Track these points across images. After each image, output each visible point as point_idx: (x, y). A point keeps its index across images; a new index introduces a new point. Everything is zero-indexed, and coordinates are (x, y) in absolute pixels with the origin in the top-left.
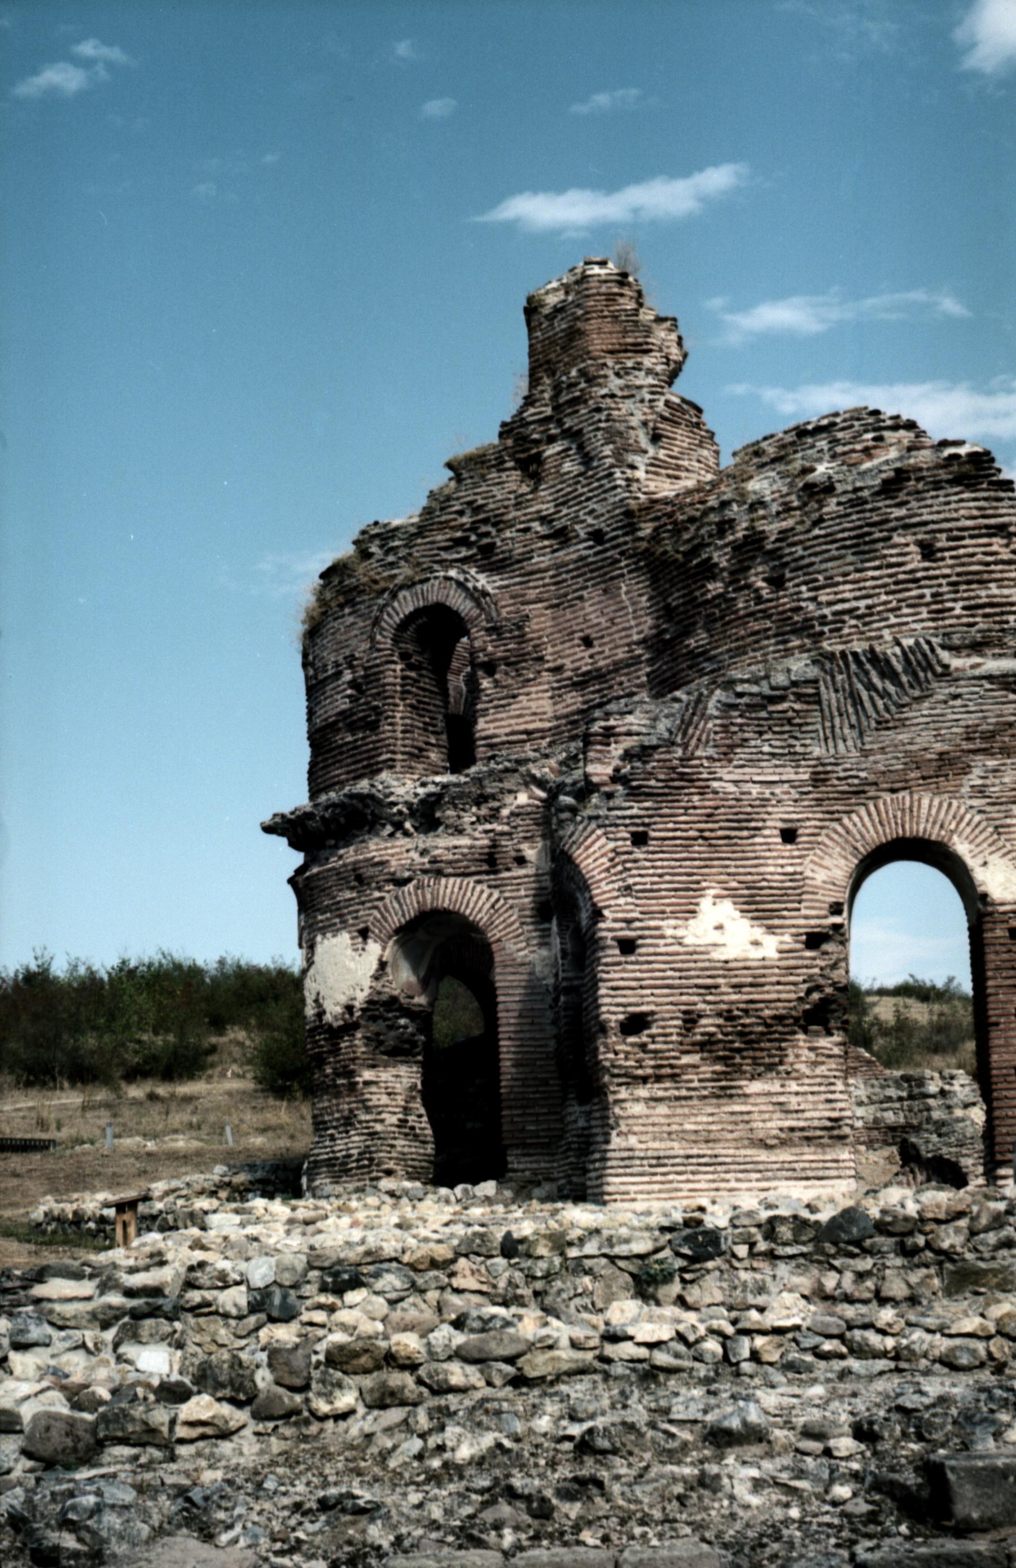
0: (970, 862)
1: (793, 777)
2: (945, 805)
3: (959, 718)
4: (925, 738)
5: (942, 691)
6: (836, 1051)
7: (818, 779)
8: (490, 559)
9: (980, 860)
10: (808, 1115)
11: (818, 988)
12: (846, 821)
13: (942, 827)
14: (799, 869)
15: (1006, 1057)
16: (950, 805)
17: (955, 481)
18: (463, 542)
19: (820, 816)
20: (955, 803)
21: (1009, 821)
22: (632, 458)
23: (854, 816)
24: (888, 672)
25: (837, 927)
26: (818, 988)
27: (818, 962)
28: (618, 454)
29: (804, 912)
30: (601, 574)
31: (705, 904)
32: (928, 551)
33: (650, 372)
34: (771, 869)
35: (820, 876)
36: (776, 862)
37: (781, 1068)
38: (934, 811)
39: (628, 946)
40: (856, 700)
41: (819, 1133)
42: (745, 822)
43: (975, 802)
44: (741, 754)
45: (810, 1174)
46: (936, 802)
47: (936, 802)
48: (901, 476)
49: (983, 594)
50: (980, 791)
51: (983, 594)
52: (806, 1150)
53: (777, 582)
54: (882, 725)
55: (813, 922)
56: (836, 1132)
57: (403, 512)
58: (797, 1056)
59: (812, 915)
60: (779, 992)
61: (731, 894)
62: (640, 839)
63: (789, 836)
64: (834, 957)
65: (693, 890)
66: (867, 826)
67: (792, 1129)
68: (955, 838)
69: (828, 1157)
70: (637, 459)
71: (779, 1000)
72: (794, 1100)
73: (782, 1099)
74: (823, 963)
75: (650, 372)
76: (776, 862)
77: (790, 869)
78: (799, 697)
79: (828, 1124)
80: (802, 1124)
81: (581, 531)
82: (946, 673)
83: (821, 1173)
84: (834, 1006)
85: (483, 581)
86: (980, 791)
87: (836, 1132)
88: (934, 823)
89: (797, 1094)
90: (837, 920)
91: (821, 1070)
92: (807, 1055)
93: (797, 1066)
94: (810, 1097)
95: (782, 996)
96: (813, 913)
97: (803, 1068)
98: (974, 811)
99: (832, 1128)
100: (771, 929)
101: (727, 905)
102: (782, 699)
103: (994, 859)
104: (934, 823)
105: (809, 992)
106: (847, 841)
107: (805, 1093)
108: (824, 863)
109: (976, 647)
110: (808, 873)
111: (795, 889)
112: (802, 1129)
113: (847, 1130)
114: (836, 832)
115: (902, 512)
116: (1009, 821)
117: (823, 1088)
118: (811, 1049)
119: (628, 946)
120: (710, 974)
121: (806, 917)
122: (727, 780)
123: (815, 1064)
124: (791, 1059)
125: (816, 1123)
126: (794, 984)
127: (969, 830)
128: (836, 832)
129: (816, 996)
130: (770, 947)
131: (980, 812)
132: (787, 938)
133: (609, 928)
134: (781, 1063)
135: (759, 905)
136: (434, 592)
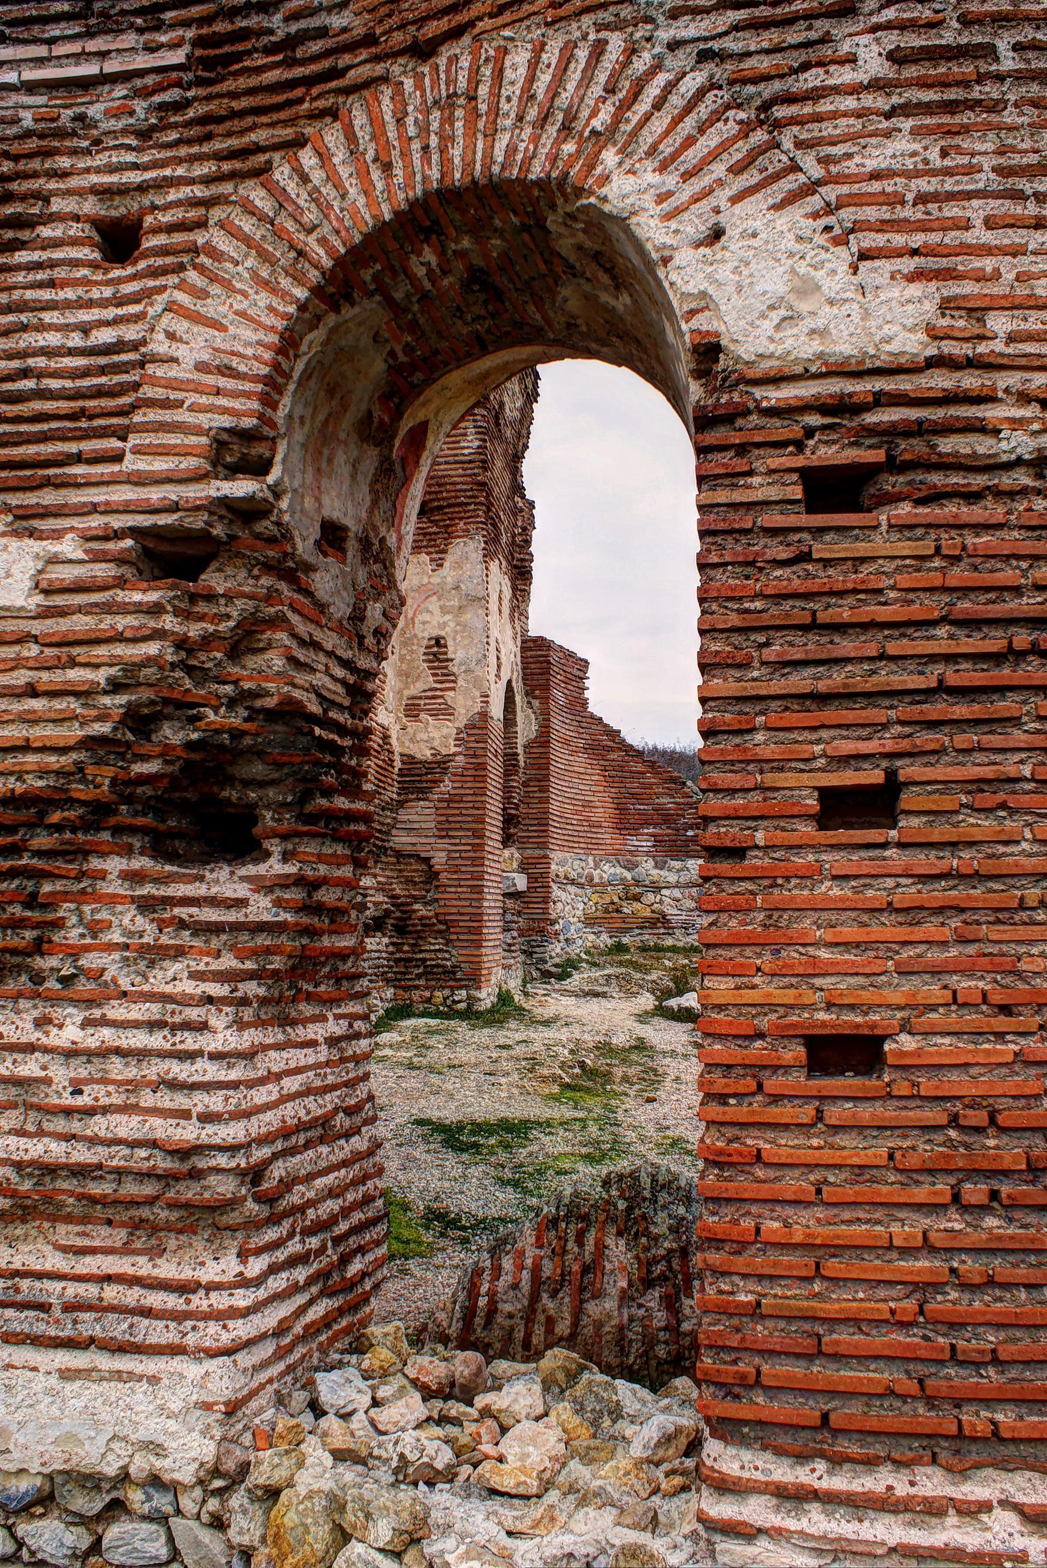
0: (652, 230)
1: (142, 61)
2: (582, 54)
6: (261, 908)
9: (694, 225)
10: (99, 1126)
11: (184, 709)
12: (282, 174)
13: (566, 129)
14: (131, 333)
15: (766, 989)
16: (599, 49)
19: (201, 170)
20: (616, 42)
21: (812, 79)
23: (307, 158)
25: (245, 512)
26: (184, 709)
27: (169, 622)
29: (131, 463)
34: (53, 339)
35: (194, 348)
37: (40, 963)
38: (544, 79)
41: (131, 1188)
43: (689, 29)
45: (89, 1325)
46: (551, 56)
47: (551, 56)
52: (101, 1236)
55: (154, 494)
56: (189, 1191)
58: (95, 928)
59: (157, 475)
60: (32, 719)
63: (118, 241)
64: (236, 610)
67: (49, 1170)
68: (610, 157)
69: (166, 1269)
71: (26, 747)
72: (60, 1074)
73: (30, 1067)
74: (194, 630)
77: (105, 336)
79: (164, 1163)
80: (82, 1155)
83: (118, 1328)
84: (258, 769)
87: (189, 1191)
88: (544, 119)
89: (71, 1053)
90: (242, 487)
91: (174, 977)
92: (127, 922)
93: (90, 961)
94: (117, 1068)
96: (160, 465)
97: (110, 963)
98: (682, 59)
99: (169, 1178)
103: (750, 216)
104: (544, 119)
105: (140, 722)
106: (278, 234)
107: (105, 1052)
108: (211, 308)
110: (159, 345)
112: (81, 1171)
113: (225, 1187)
114: (250, 209)
116: (812, 79)
117: (157, 1040)
118: (146, 906)
121: (139, 480)
123: (155, 955)
124: (73, 935)
125: (118, 1157)
126: (84, 693)
127: (659, 124)
128: (250, 209)
129: (173, 734)
131: (704, 56)
132: (69, 547)
134: (39, 947)
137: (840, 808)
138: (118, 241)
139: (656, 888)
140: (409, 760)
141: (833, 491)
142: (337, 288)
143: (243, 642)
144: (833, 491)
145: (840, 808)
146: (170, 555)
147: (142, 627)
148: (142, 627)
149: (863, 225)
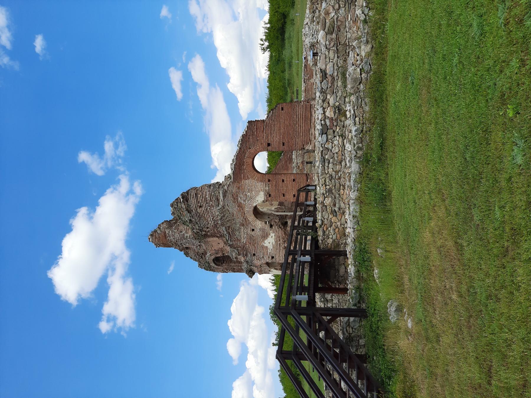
3: (231, 204)
4: (235, 209)
5: (227, 207)
7: (243, 225)
8: (204, 254)
17: (187, 202)
18: (201, 257)
22: (185, 237)
24: (224, 216)
28: (185, 239)
30: (206, 243)
31: (265, 245)
32: (201, 207)
33: (169, 232)
35: (260, 225)
36: (258, 232)
39: (273, 257)
40: (228, 221)
42: (251, 238)
44: (239, 238)
48: (187, 210)
49: (208, 198)
50: (244, 201)
51: (208, 198)
53: (207, 228)
54: (233, 216)
57: (197, 263)
59: (267, 227)
61: (264, 240)
62: (254, 255)
63: (253, 230)
65: (263, 247)
66: (251, 217)
70: (186, 235)
75: (169, 232)
76: (258, 232)
78: (229, 229)
81: (199, 244)
82: (223, 207)
85: (208, 254)
86: (244, 201)
95: (281, 233)
100: (269, 234)
101: (266, 241)
102: (229, 232)
109: (218, 200)
111: (262, 230)
115: (194, 211)
119: (273, 257)
120: (277, 245)
122: (244, 240)
130: (273, 235)
133: (270, 261)
135: (265, 236)
136: (211, 261)
137: (284, 196)
138: (253, 230)
139: (297, 163)
140: (279, 205)
141: (270, 196)
142: (257, 218)
143: (276, 222)
144: (270, 196)
145: (284, 196)
146: (271, 226)
147: (275, 227)
148: (275, 227)
149: (257, 194)
